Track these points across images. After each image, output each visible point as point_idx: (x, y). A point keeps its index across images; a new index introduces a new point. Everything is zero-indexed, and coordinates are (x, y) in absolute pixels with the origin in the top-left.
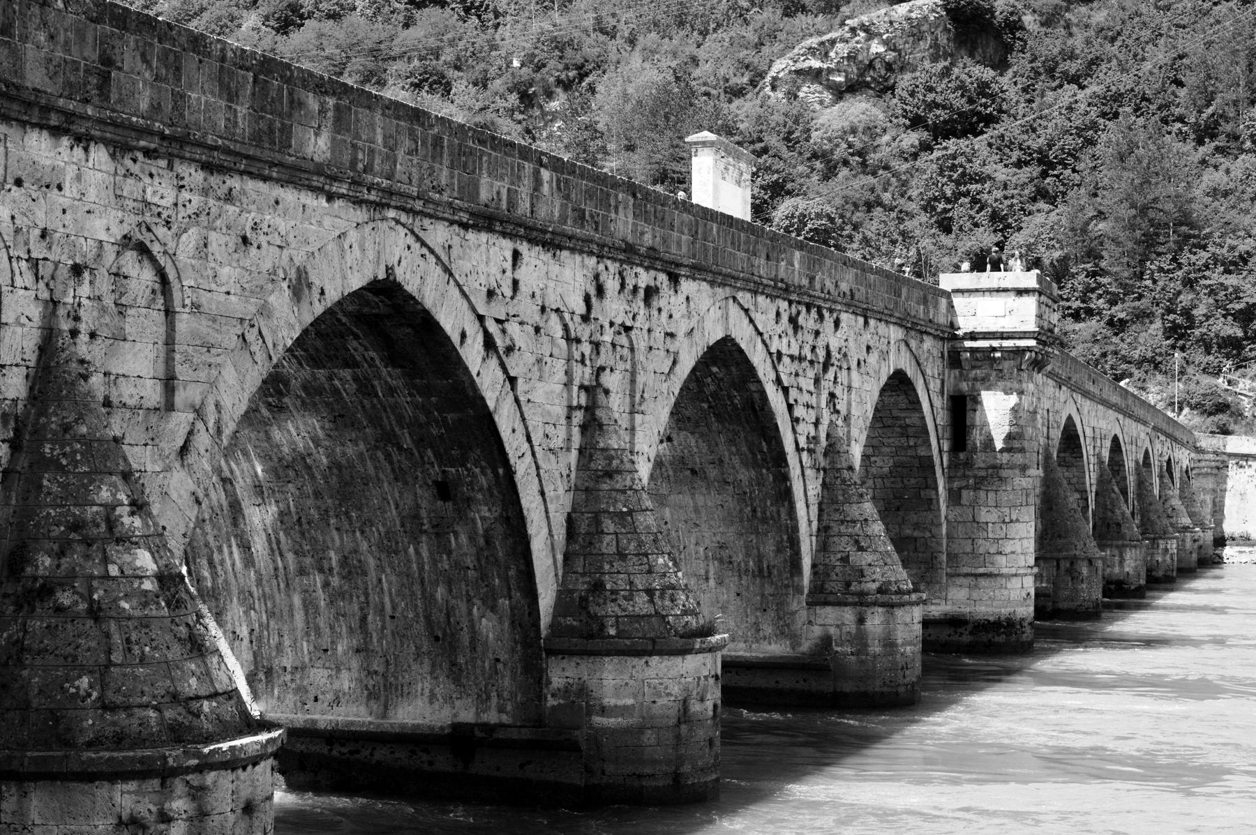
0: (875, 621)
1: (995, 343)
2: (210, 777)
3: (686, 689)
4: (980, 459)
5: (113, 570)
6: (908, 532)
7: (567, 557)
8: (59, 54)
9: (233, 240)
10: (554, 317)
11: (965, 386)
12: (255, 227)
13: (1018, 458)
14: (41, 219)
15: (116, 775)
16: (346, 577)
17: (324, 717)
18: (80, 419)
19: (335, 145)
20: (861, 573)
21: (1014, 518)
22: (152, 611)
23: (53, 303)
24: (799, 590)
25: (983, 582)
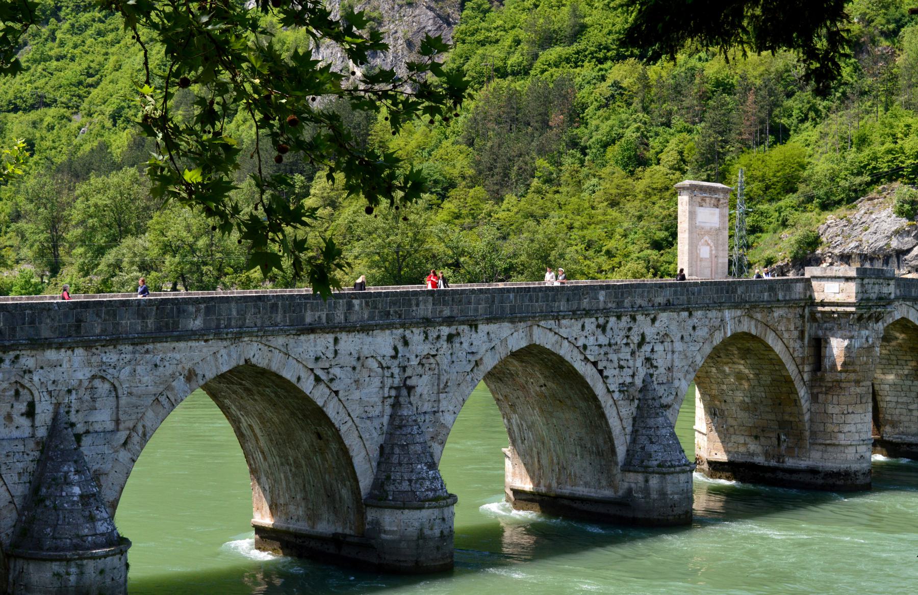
0: (654, 481)
1: (834, 309)
2: (85, 562)
3: (422, 524)
4: (829, 377)
5: (64, 494)
6: (787, 417)
7: (379, 464)
8: (56, 324)
9: (149, 368)
10: (370, 360)
11: (820, 333)
12: (162, 360)
13: (852, 376)
14: (52, 377)
15: (52, 560)
16: (297, 467)
17: (293, 526)
18: (62, 443)
19: (205, 321)
20: (650, 456)
21: (850, 411)
22: (76, 507)
23: (58, 405)
24: (616, 464)
25: (830, 449)
